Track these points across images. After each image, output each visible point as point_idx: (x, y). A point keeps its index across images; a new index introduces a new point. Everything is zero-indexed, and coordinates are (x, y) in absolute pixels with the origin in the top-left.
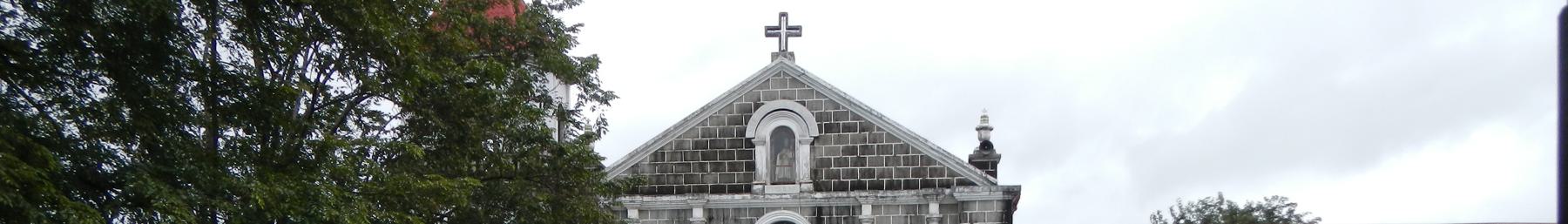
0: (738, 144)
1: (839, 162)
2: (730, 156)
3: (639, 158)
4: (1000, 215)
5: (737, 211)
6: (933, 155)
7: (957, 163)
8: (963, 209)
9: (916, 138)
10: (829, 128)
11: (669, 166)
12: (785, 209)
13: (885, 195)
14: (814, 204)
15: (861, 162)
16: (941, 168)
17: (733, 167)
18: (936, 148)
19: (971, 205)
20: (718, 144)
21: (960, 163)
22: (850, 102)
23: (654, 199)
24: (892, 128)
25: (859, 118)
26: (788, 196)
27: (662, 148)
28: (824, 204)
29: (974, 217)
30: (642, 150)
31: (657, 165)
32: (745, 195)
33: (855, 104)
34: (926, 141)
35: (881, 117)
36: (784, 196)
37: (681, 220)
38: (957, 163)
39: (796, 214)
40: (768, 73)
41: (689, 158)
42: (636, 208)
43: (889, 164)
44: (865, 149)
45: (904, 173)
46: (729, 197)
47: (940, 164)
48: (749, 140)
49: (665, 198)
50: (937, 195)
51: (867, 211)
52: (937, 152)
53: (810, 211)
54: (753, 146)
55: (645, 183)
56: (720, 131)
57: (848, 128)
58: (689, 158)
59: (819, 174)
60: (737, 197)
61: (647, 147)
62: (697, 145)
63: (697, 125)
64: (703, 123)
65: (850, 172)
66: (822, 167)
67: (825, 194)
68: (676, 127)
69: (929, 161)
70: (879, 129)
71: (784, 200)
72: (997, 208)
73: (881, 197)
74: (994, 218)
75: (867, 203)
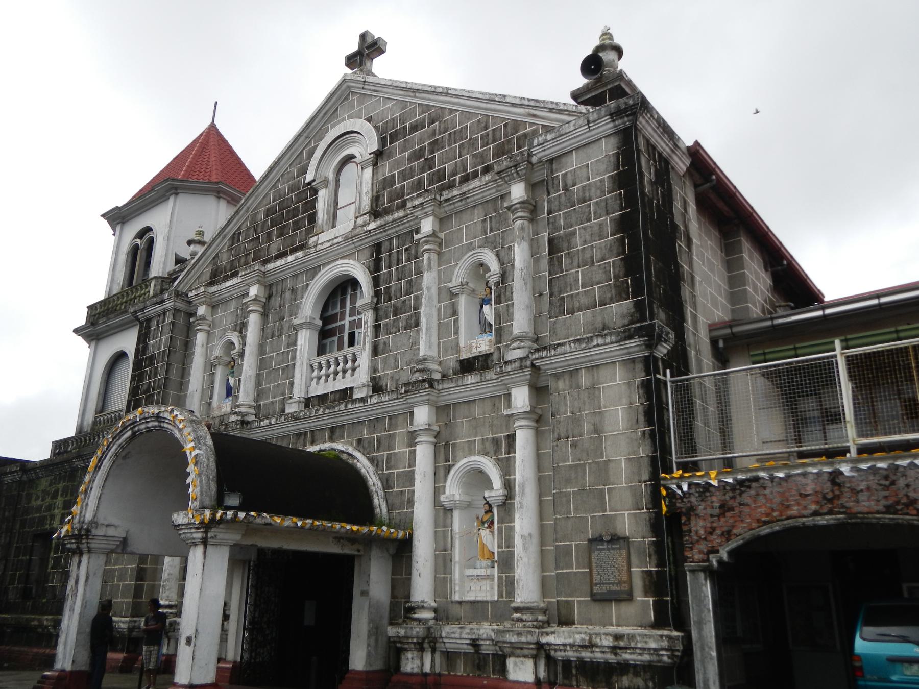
0: (304, 196)
1: (404, 176)
3: (218, 245)
4: (612, 159)
5: (295, 278)
6: (518, 114)
7: (551, 110)
8: (552, 172)
9: (491, 99)
10: (394, 137)
12: (342, 258)
13: (450, 196)
14: (370, 241)
15: (429, 164)
17: (297, 226)
18: (517, 102)
19: (564, 160)
20: (285, 205)
21: (554, 108)
24: (462, 101)
26: (340, 239)
27: (239, 228)
28: (382, 237)
29: (569, 182)
30: (219, 235)
32: (297, 254)
33: (418, 91)
34: (505, 96)
35: (446, 92)
38: (551, 110)
39: (351, 262)
40: (334, 99)
41: (259, 230)
43: (463, 154)
44: (435, 145)
45: (482, 157)
46: (281, 262)
47: (531, 124)
49: (228, 284)
50: (515, 166)
51: (427, 226)
52: (520, 106)
53: (367, 253)
54: (316, 192)
55: (221, 272)
56: (289, 188)
57: (415, 128)
59: (381, 197)
60: (290, 258)
62: (268, 212)
64: (275, 186)
65: (415, 183)
66: (384, 189)
67: (379, 222)
69: (517, 125)
70: (451, 111)
71: (336, 247)
72: (607, 149)
73: (447, 200)
74: (602, 167)
75: (427, 215)
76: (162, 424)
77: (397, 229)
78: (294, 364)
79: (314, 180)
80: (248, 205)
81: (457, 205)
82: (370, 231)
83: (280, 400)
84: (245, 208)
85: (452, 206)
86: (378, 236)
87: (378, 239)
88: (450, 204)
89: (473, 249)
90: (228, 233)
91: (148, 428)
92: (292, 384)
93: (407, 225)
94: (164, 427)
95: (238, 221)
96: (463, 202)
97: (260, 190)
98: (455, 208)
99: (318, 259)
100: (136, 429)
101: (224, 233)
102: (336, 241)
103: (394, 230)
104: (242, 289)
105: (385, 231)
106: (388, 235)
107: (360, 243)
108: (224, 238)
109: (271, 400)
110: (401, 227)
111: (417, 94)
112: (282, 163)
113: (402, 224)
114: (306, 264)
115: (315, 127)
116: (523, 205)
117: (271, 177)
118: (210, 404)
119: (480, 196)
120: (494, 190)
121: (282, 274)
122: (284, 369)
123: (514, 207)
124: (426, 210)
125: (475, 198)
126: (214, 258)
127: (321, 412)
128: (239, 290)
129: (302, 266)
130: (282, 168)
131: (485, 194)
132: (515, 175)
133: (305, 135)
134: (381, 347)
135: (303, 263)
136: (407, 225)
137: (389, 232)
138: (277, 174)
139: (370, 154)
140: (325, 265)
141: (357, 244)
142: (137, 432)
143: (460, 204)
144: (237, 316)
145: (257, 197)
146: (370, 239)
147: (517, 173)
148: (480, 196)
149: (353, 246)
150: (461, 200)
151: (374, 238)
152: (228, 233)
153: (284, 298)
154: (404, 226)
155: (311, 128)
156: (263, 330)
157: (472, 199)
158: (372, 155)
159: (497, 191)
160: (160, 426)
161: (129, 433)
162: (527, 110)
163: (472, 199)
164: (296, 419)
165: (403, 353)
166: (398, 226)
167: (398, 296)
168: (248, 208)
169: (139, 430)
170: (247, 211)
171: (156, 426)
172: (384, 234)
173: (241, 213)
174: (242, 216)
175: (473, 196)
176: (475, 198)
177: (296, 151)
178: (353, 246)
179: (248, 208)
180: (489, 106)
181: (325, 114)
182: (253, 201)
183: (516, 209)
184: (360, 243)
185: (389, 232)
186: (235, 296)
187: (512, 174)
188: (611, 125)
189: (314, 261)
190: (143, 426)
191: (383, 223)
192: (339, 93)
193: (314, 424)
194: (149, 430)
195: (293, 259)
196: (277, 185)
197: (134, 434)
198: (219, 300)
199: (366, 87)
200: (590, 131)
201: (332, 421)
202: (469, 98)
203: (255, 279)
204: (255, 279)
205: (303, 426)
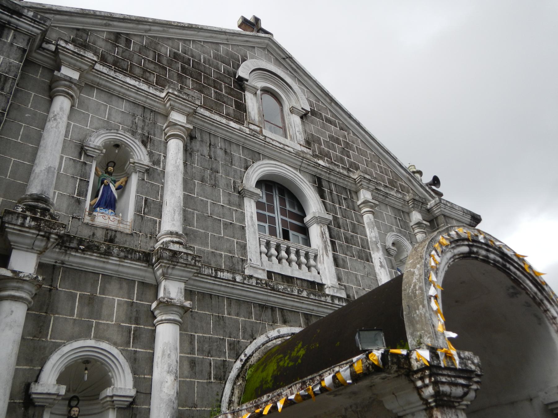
2: (216, 85)
3: (93, 24)
11: (136, 57)
16: (408, 188)
20: (202, 68)
22: (332, 100)
23: (112, 73)
25: (336, 117)
26: (292, 150)
28: (324, 175)
31: (118, 46)
33: (337, 104)
36: (286, 147)
37: (147, 121)
42: (79, 69)
48: (241, 79)
54: (243, 89)
58: (165, 62)
61: (110, 18)
63: (178, 39)
68: (155, 23)
70: (354, 134)
75: (368, 189)
76: (508, 265)
77: (338, 180)
78: (243, 228)
79: (247, 80)
80: (153, 28)
81: (380, 196)
82: (319, 165)
83: (226, 256)
84: (148, 27)
85: (377, 195)
86: (323, 173)
87: (320, 174)
88: (377, 193)
89: (393, 231)
90: (114, 26)
91: (487, 257)
92: (243, 247)
93: (346, 183)
94: (509, 269)
95: (132, 28)
96: (384, 198)
97: (171, 30)
98: (378, 197)
99: (263, 148)
100: (475, 250)
101: (111, 23)
102: (286, 147)
103: (335, 178)
104: (148, 101)
105: (329, 174)
106: (329, 178)
107: (306, 166)
108: (106, 25)
109: (209, 249)
110: (341, 181)
111: (333, 104)
112: (201, 33)
113: (343, 180)
114: (247, 142)
115: (235, 40)
116: (417, 226)
117: (184, 32)
118: (79, 202)
119: (393, 202)
120: (401, 205)
121: (214, 128)
122: (225, 224)
123: (423, 225)
124: (370, 186)
125: (391, 201)
126: (78, 30)
127: (305, 294)
128: (144, 99)
129: (243, 140)
130: (198, 36)
131: (396, 203)
132: (420, 207)
133: (228, 37)
134: (341, 262)
135: (245, 139)
136: (346, 183)
137: (332, 177)
138: (191, 35)
139: (302, 109)
140: (266, 157)
141: (303, 165)
142: (473, 253)
143: (381, 197)
144: (134, 123)
145: (164, 31)
146: (316, 170)
147: (421, 207)
148: (393, 202)
149: (300, 164)
150: (383, 196)
151: (319, 171)
152: (114, 26)
153: (214, 152)
154: (343, 181)
155: (235, 38)
156: (185, 164)
157: (389, 200)
158: (304, 111)
159: (402, 207)
160: (505, 266)
161: (465, 249)
162: (408, 175)
163: (389, 200)
164: (273, 289)
165: (362, 276)
166: (340, 178)
167: (346, 229)
168: (150, 30)
169: (477, 253)
170: (146, 31)
171: (498, 262)
172: (327, 175)
173: (141, 26)
174: (139, 30)
175: (390, 199)
176: (391, 201)
177: (215, 38)
178: (300, 164)
179: (150, 30)
180: (384, 154)
181: (247, 41)
182: (158, 31)
183: (423, 226)
184: (306, 166)
185: (332, 177)
186: (132, 99)
187: (419, 206)
188: (469, 220)
189: (257, 146)
190: (483, 252)
191: (332, 168)
192: (262, 41)
193: (289, 303)
194: (486, 260)
195: (238, 128)
196: (187, 42)
197: (471, 252)
198: (98, 84)
199: (287, 60)
200: (463, 216)
201: (311, 308)
202: (373, 139)
203: (188, 110)
204: (188, 110)
205: (276, 300)
